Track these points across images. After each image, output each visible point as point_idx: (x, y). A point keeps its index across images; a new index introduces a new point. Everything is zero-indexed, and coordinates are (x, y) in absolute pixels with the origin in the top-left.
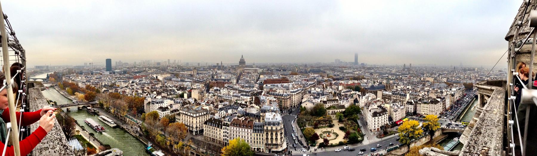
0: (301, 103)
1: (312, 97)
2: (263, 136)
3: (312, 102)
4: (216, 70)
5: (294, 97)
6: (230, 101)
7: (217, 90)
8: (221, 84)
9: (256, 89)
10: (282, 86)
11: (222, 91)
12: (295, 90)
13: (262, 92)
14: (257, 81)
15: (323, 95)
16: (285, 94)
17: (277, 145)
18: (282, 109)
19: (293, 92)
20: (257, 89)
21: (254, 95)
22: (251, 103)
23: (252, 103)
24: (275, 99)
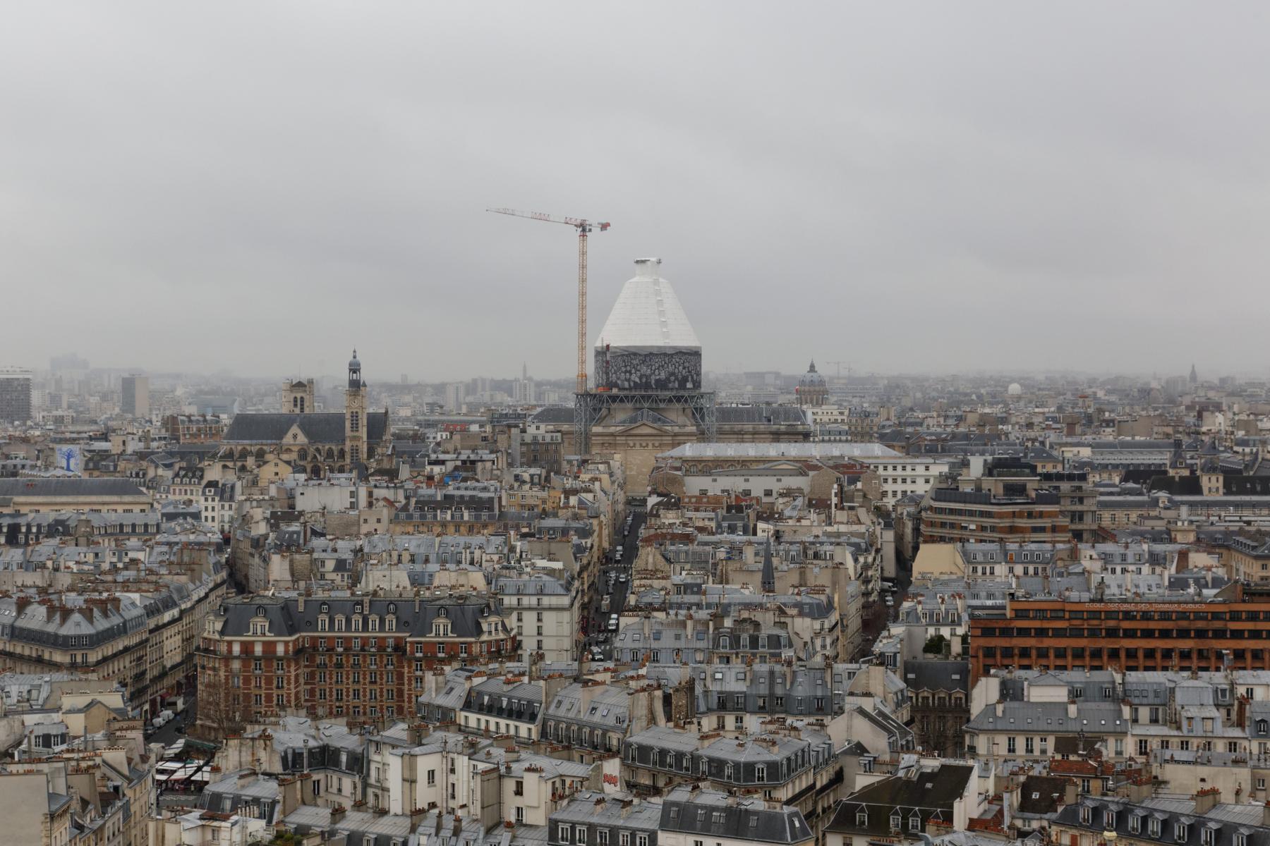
7: (325, 757)
10: (1237, 709)
13: (955, 781)
20: (877, 742)
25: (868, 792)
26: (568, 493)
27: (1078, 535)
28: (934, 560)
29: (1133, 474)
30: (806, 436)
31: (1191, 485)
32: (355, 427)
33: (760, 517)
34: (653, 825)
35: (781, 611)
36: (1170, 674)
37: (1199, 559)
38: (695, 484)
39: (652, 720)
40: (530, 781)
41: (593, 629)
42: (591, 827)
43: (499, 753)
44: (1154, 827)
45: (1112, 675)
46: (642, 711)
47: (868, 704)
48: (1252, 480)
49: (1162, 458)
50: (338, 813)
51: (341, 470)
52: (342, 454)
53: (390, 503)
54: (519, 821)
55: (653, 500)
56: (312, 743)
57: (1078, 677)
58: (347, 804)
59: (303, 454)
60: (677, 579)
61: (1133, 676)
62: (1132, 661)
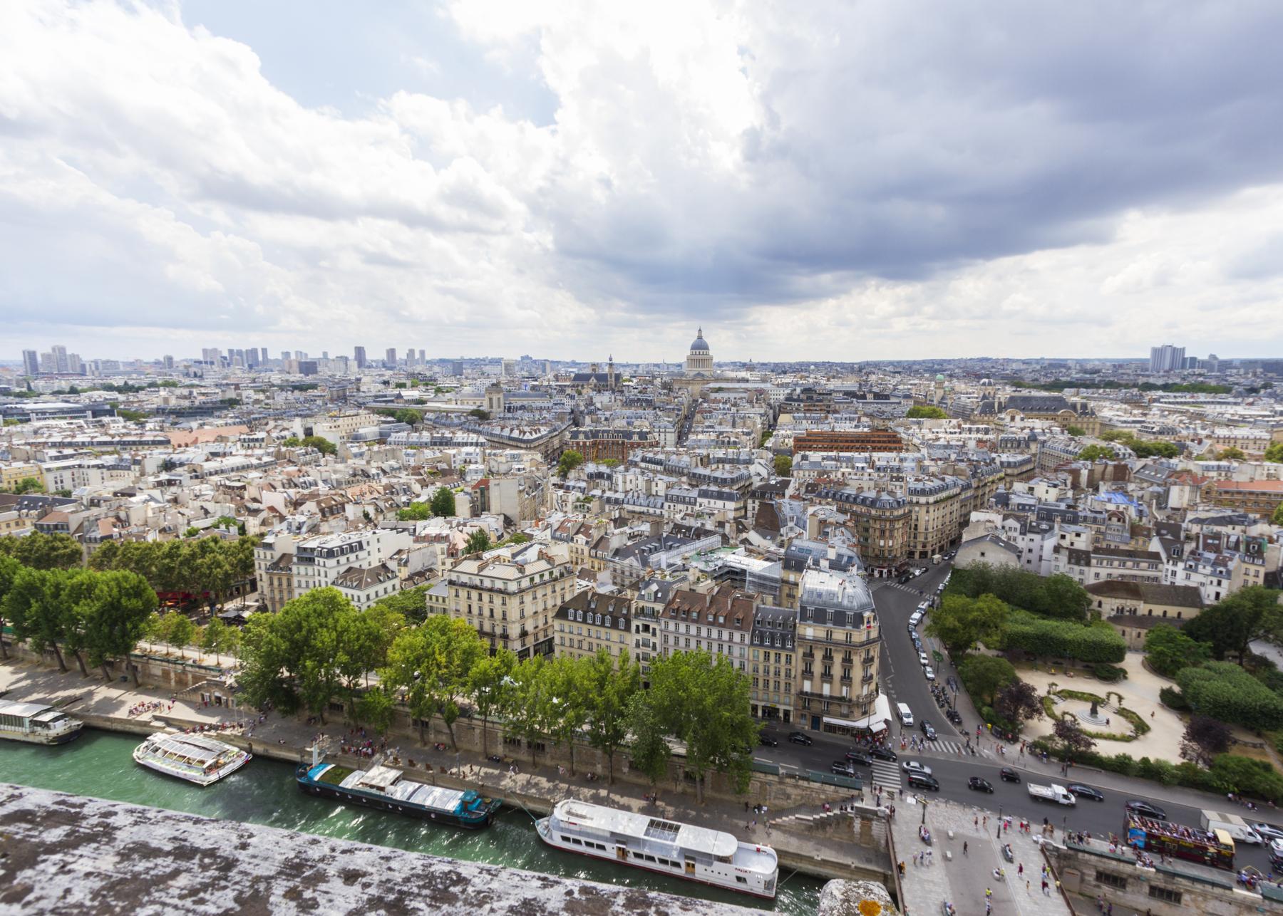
0: (955, 542)
1: (1012, 523)
3: (1010, 547)
4: (587, 392)
6: (657, 522)
8: (616, 448)
9: (760, 471)
10: (872, 464)
11: (619, 478)
12: (929, 485)
13: (786, 484)
14: (766, 435)
15: (1071, 517)
16: (885, 496)
18: (872, 562)
19: (923, 492)
21: (753, 495)
22: (741, 528)
23: (745, 529)
24: (842, 518)
25: (760, 487)
29: (847, 393)
31: (864, 397)
37: (864, 419)
38: (713, 396)
41: (681, 438)
43: (651, 475)
45: (833, 454)
47: (762, 461)
50: (604, 491)
57: (825, 454)
60: (707, 424)
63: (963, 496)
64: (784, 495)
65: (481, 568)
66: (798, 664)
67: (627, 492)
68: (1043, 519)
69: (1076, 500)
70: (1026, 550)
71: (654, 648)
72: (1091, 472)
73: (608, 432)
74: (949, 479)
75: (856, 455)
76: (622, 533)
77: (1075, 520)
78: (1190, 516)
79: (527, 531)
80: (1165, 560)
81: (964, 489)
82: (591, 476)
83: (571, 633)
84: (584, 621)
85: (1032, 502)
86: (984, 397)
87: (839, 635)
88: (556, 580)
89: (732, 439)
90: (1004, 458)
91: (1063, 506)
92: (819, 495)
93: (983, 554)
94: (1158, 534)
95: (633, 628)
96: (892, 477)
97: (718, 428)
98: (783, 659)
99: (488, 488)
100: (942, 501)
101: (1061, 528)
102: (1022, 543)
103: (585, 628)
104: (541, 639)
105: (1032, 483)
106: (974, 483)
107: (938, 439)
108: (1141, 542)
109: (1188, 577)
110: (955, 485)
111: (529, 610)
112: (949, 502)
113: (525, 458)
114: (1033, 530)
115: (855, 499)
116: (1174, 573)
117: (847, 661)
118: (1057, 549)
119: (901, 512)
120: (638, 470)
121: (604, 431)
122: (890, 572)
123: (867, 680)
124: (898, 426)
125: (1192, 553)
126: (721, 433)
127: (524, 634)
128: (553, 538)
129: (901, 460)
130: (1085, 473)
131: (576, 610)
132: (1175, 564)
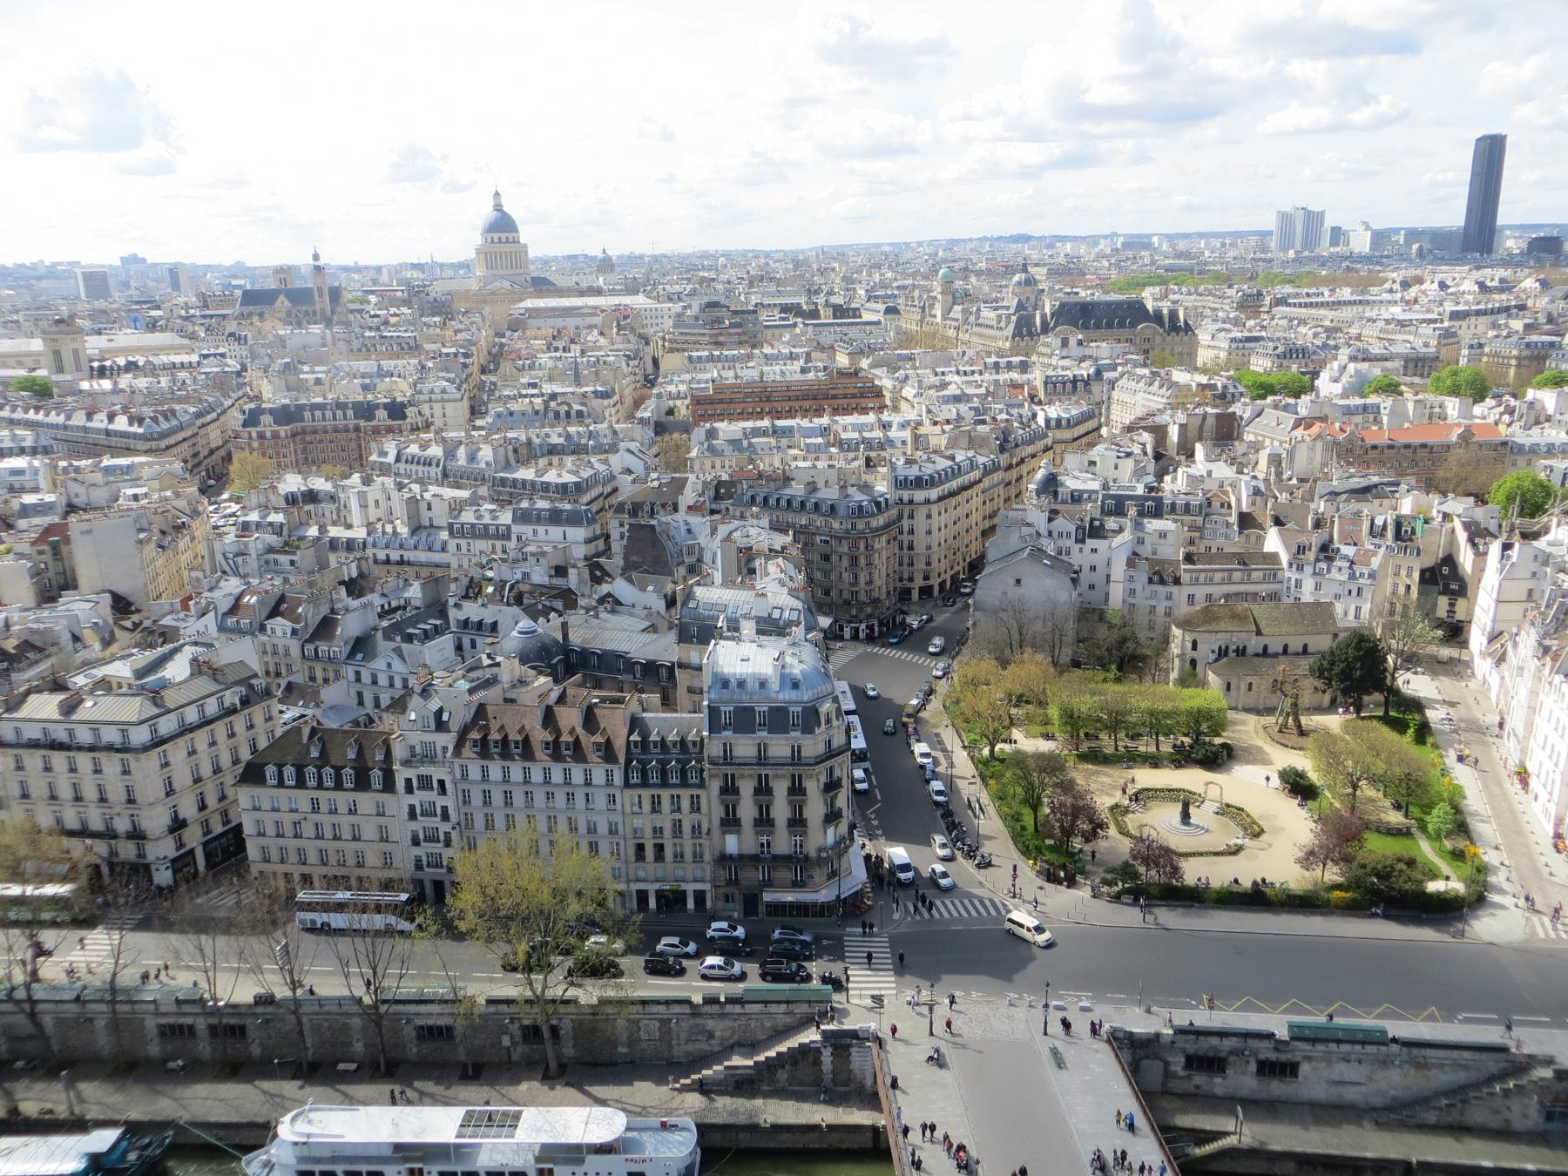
0: (976, 566)
2: (696, 807)
3: (1059, 563)
5: (921, 513)
12: (929, 469)
13: (680, 485)
17: (800, 865)
22: (598, 573)
26: (456, 332)
27: (754, 347)
28: (669, 362)
29: (785, 309)
30: (598, 292)
31: (814, 314)
32: (321, 294)
33: (572, 341)
34: (509, 522)
35: (584, 395)
36: (798, 420)
39: (508, 463)
40: (435, 504)
42: (473, 525)
43: (416, 488)
44: (783, 503)
45: (765, 423)
46: (501, 458)
47: (633, 446)
48: (848, 310)
49: (802, 300)
51: (315, 323)
52: (315, 313)
53: (348, 342)
54: (431, 526)
55: (508, 334)
56: (303, 488)
57: (749, 424)
58: (329, 522)
59: (289, 314)
60: (524, 381)
61: (780, 423)
62: (779, 415)
63: (987, 482)
64: (676, 510)
65: (69, 709)
66: (713, 807)
67: (370, 527)
68: (1110, 513)
69: (1160, 476)
70: (1086, 569)
71: (445, 816)
72: (1183, 428)
73: (322, 407)
74: (960, 456)
75: (805, 423)
76: (365, 606)
77: (1157, 513)
78: (1322, 487)
79: (167, 621)
80: (1285, 564)
81: (987, 472)
82: (291, 500)
83: (275, 810)
84: (301, 784)
85: (1095, 485)
86: (1020, 306)
87: (779, 747)
88: (232, 711)
89: (576, 407)
90: (1054, 411)
91: (1140, 490)
92: (739, 503)
93: (1018, 581)
94: (1278, 522)
95: (400, 784)
96: (868, 460)
97: (547, 388)
98: (685, 804)
99: (67, 540)
100: (952, 494)
101: (1138, 526)
102: (1080, 556)
103: (303, 798)
104: (218, 829)
105: (1096, 452)
106: (1004, 459)
107: (944, 385)
108: (1253, 539)
109: (1318, 587)
110: (973, 465)
111: (182, 778)
112: (965, 494)
113: (146, 473)
114: (1097, 532)
115: (803, 503)
116: (1298, 584)
117: (797, 790)
118: (1133, 560)
119: (879, 521)
120: (389, 481)
121: (314, 407)
122: (871, 628)
123: (832, 817)
124: (873, 366)
125: (1325, 548)
126: (553, 396)
127: (178, 825)
128: (222, 628)
129: (886, 426)
130: (1174, 434)
131: (280, 766)
132: (1300, 568)
